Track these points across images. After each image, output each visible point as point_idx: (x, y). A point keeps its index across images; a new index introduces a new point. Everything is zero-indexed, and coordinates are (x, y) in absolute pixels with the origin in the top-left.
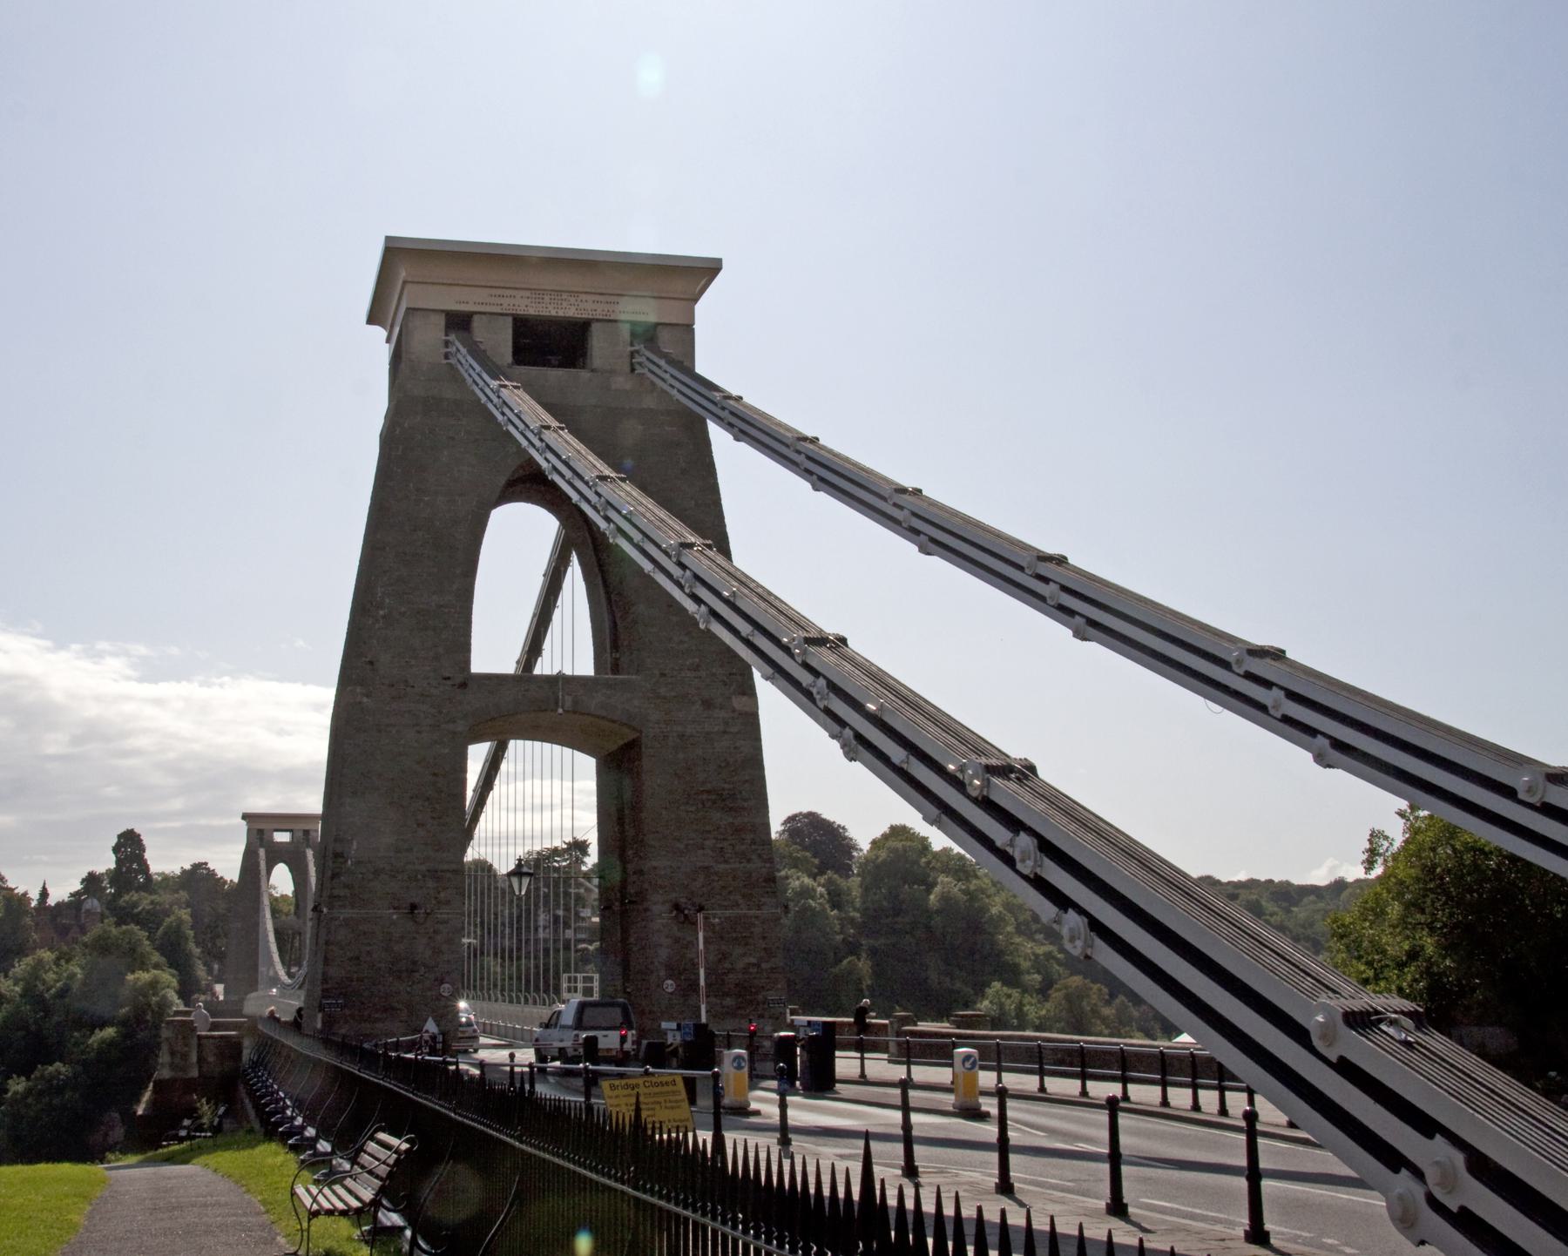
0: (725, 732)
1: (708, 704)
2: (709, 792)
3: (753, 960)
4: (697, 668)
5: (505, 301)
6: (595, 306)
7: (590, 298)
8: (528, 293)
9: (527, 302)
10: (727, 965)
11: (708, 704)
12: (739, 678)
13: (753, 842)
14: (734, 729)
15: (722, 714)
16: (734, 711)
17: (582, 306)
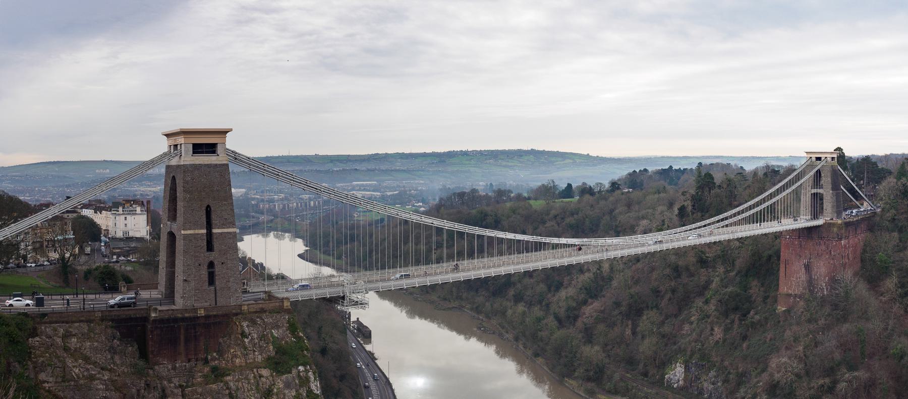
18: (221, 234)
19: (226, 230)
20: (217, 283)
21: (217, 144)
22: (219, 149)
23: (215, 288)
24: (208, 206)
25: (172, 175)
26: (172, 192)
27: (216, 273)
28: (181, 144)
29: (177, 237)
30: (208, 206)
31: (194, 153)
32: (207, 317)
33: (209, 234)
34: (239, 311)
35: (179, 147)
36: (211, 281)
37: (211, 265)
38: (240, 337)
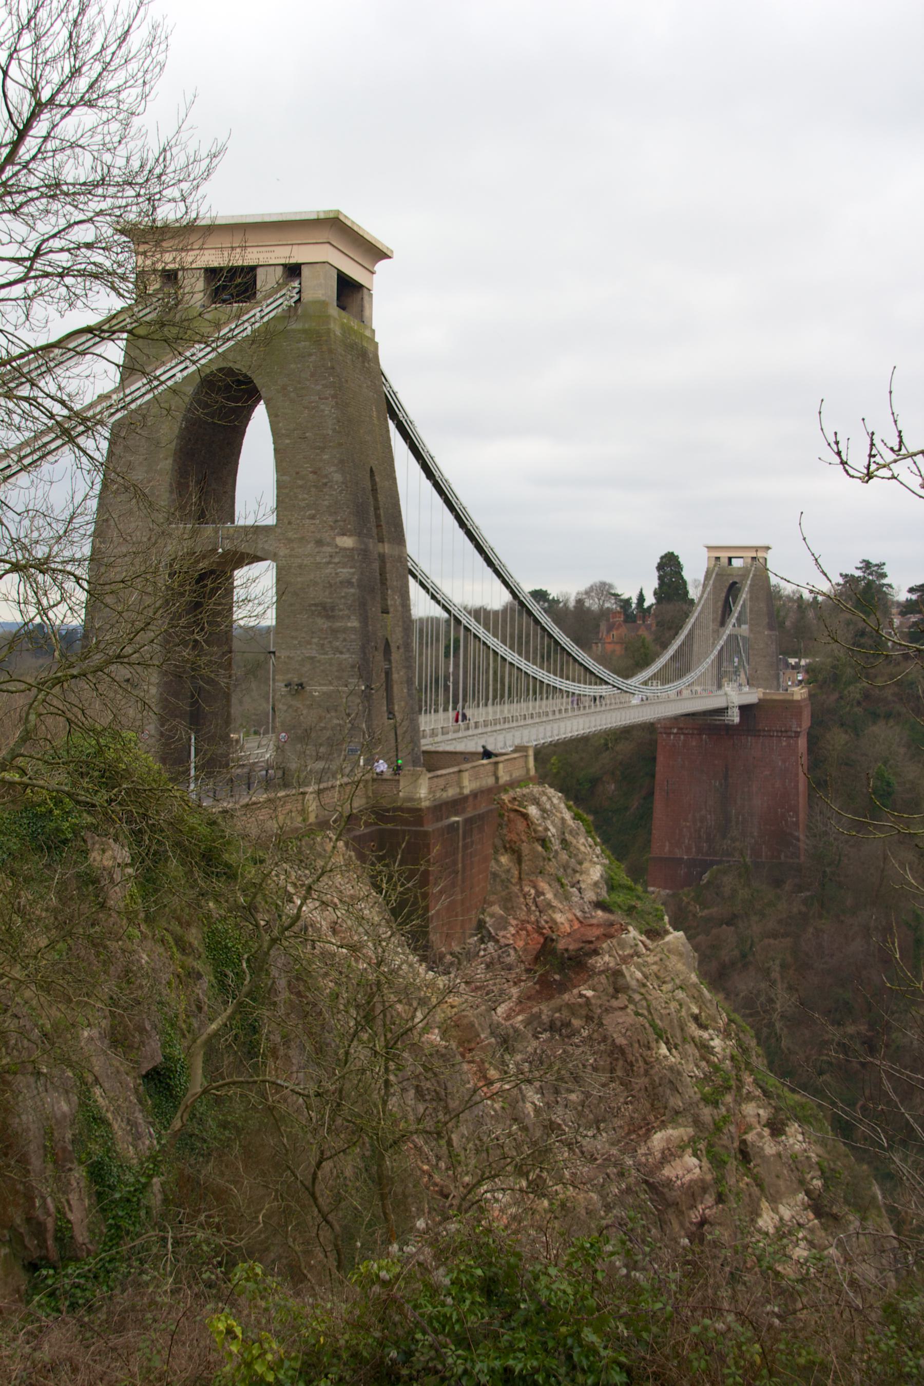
0: (329, 563)
1: (319, 543)
2: (315, 605)
4: (313, 517)
6: (259, 256)
7: (255, 250)
8: (213, 251)
9: (213, 258)
10: (322, 725)
11: (319, 543)
12: (342, 523)
13: (345, 640)
14: (336, 560)
15: (328, 549)
16: (337, 546)
17: (250, 256)
28: (293, 271)
34: (491, 781)
38: (540, 849)
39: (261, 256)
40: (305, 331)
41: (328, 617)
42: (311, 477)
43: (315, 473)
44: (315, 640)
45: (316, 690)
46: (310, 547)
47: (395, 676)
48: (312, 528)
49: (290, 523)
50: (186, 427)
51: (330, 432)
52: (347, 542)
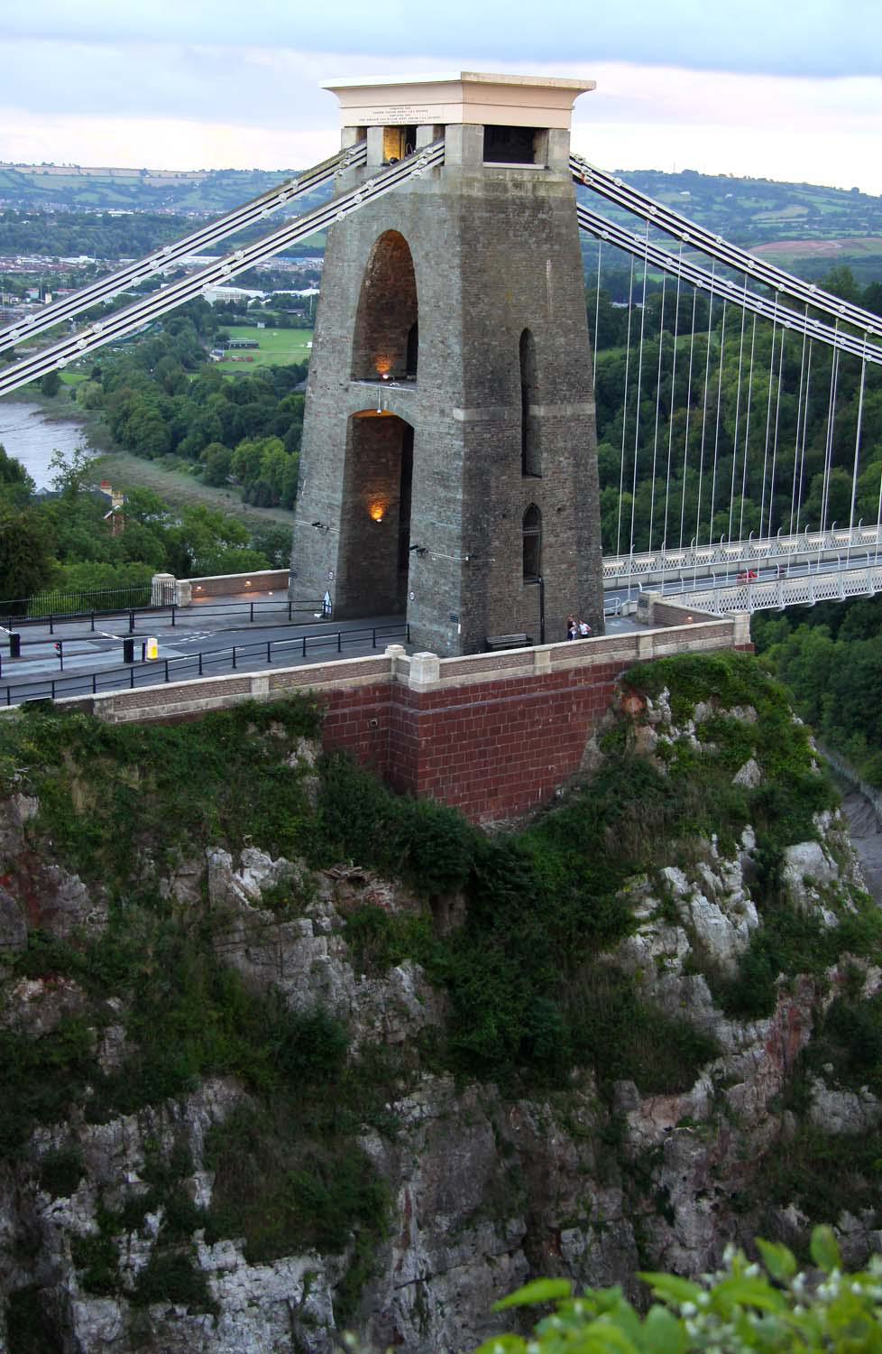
2: (437, 473)
3: (447, 589)
5: (380, 116)
11: (442, 412)
14: (452, 432)
15: (447, 420)
18: (559, 421)
19: (569, 411)
20: (547, 571)
21: (544, 130)
22: (556, 153)
23: (542, 586)
24: (526, 334)
25: (377, 229)
26: (368, 283)
27: (544, 541)
28: (440, 129)
29: (417, 429)
30: (526, 334)
31: (489, 155)
32: (560, 677)
33: (527, 424)
35: (424, 137)
36: (531, 571)
37: (532, 515)
38: (652, 732)
39: (418, 115)
40: (444, 197)
41: (446, 487)
42: (441, 345)
43: (442, 342)
44: (436, 507)
45: (436, 556)
46: (436, 417)
47: (548, 539)
48: (439, 398)
49: (425, 390)
50: (372, 285)
51: (454, 302)
52: (460, 414)
